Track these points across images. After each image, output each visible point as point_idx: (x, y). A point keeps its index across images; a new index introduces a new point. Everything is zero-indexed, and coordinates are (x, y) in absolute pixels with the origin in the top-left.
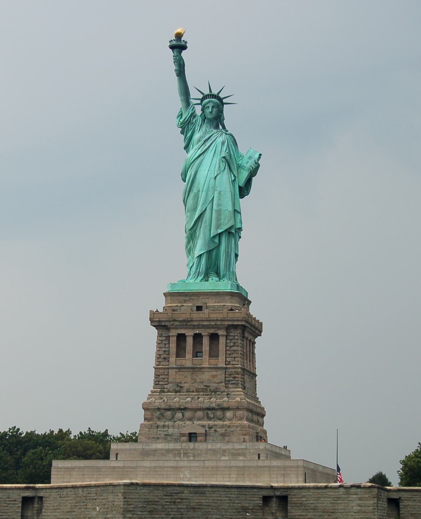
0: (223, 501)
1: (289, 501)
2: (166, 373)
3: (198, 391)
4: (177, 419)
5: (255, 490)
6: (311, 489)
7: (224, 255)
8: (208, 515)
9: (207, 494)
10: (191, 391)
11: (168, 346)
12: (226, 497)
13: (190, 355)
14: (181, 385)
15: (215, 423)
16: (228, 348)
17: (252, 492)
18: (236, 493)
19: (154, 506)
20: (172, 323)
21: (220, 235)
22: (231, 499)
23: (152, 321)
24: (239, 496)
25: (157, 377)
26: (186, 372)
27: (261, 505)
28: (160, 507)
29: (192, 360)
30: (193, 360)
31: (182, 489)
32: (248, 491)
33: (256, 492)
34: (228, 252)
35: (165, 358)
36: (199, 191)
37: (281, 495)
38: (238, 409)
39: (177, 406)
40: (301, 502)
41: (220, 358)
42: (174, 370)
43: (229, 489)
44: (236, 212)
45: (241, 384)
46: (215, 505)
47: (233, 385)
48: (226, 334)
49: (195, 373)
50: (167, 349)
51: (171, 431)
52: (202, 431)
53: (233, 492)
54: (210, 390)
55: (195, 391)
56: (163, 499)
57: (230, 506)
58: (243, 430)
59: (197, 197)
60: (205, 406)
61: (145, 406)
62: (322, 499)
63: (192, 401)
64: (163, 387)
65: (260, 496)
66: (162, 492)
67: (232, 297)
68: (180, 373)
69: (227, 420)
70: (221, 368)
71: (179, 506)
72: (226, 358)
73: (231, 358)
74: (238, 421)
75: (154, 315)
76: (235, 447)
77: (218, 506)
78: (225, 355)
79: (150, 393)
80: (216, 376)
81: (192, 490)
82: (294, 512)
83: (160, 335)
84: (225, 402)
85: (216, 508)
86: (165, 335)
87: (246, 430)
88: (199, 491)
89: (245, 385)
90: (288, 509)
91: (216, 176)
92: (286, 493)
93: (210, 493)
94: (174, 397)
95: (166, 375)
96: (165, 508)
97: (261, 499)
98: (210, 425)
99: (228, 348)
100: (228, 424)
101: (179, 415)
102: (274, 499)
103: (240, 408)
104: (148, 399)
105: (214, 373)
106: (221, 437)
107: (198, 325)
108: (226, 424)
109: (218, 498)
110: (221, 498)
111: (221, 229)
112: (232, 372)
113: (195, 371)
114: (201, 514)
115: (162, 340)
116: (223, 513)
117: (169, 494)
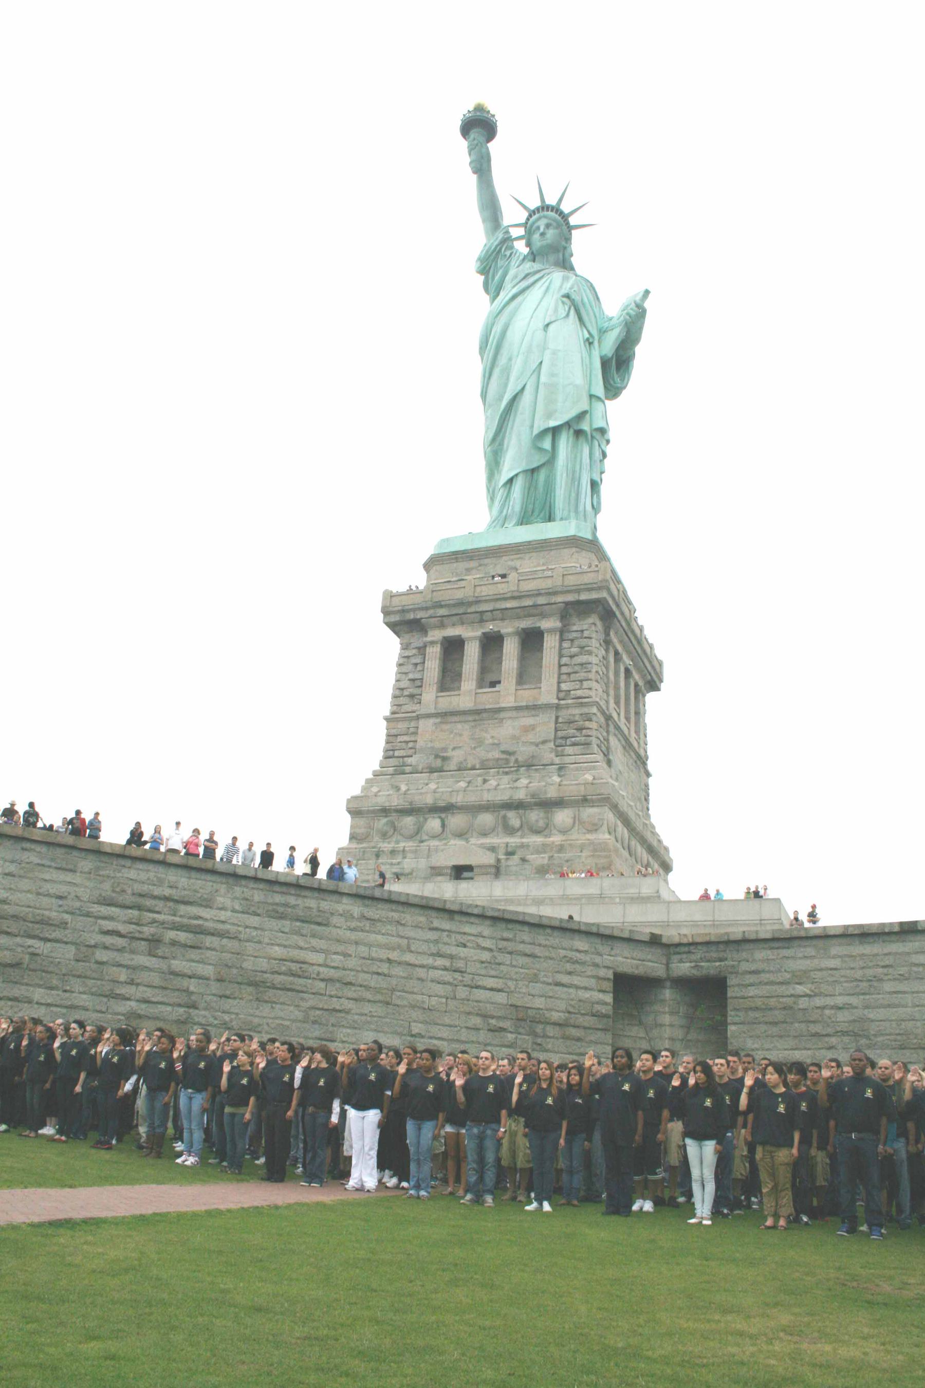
0: (421, 973)
1: (732, 998)
2: (412, 730)
3: (485, 766)
4: (427, 835)
5: (581, 944)
6: (834, 941)
7: (565, 475)
8: (333, 1025)
9: (335, 927)
10: (469, 766)
11: (421, 669)
12: (439, 955)
13: (470, 682)
14: (445, 754)
15: (524, 840)
16: (564, 660)
17: (564, 949)
18: (487, 943)
19: (30, 942)
20: (431, 612)
21: (555, 431)
22: (460, 964)
23: (386, 612)
24: (501, 958)
25: (392, 740)
26: (459, 722)
27: (604, 1010)
28: (70, 952)
29: (476, 694)
30: (477, 695)
31: (203, 885)
32: (543, 942)
33: (586, 952)
34: (574, 472)
35: (412, 696)
36: (510, 359)
37: (695, 972)
38: (585, 801)
39: (429, 800)
40: (789, 1001)
41: (544, 685)
42: (432, 721)
43: (452, 919)
44: (593, 400)
45: (597, 745)
46: (374, 982)
47: (576, 747)
48: (558, 624)
49: (479, 725)
50: (418, 676)
51: (408, 864)
52: (489, 859)
53: (473, 938)
54: (516, 761)
55: (477, 767)
56: (88, 915)
57: (455, 998)
58: (599, 856)
59: (507, 371)
60: (499, 798)
61: (353, 805)
62: (888, 987)
63: (470, 788)
64: (403, 762)
65: (602, 973)
66: (90, 884)
67: (577, 549)
68: (445, 727)
69: (557, 833)
70: (547, 707)
71: (178, 965)
72: (559, 683)
73: (573, 683)
74: (585, 833)
75: (394, 599)
76: (569, 892)
77: (393, 990)
78: (556, 676)
79: (372, 776)
80: (533, 728)
81: (258, 896)
82: (756, 1046)
83: (405, 647)
84: (551, 786)
85: (379, 997)
86: (413, 645)
87: (606, 857)
88: (294, 907)
89: (611, 757)
90: (729, 1033)
91: (547, 325)
92: (717, 964)
93: (353, 924)
94: (426, 781)
95: (413, 733)
96: (97, 962)
97: (609, 986)
98: (509, 845)
99: (564, 660)
100: (557, 841)
101: (434, 824)
102: (667, 994)
103: (592, 801)
104: (364, 789)
105: (530, 721)
106: (537, 875)
107: (491, 611)
108: (553, 842)
109: (394, 955)
110: (409, 957)
111: (556, 419)
112: (574, 715)
113: (481, 720)
114: (299, 1015)
115: (408, 657)
116: (416, 1028)
117: (129, 899)
